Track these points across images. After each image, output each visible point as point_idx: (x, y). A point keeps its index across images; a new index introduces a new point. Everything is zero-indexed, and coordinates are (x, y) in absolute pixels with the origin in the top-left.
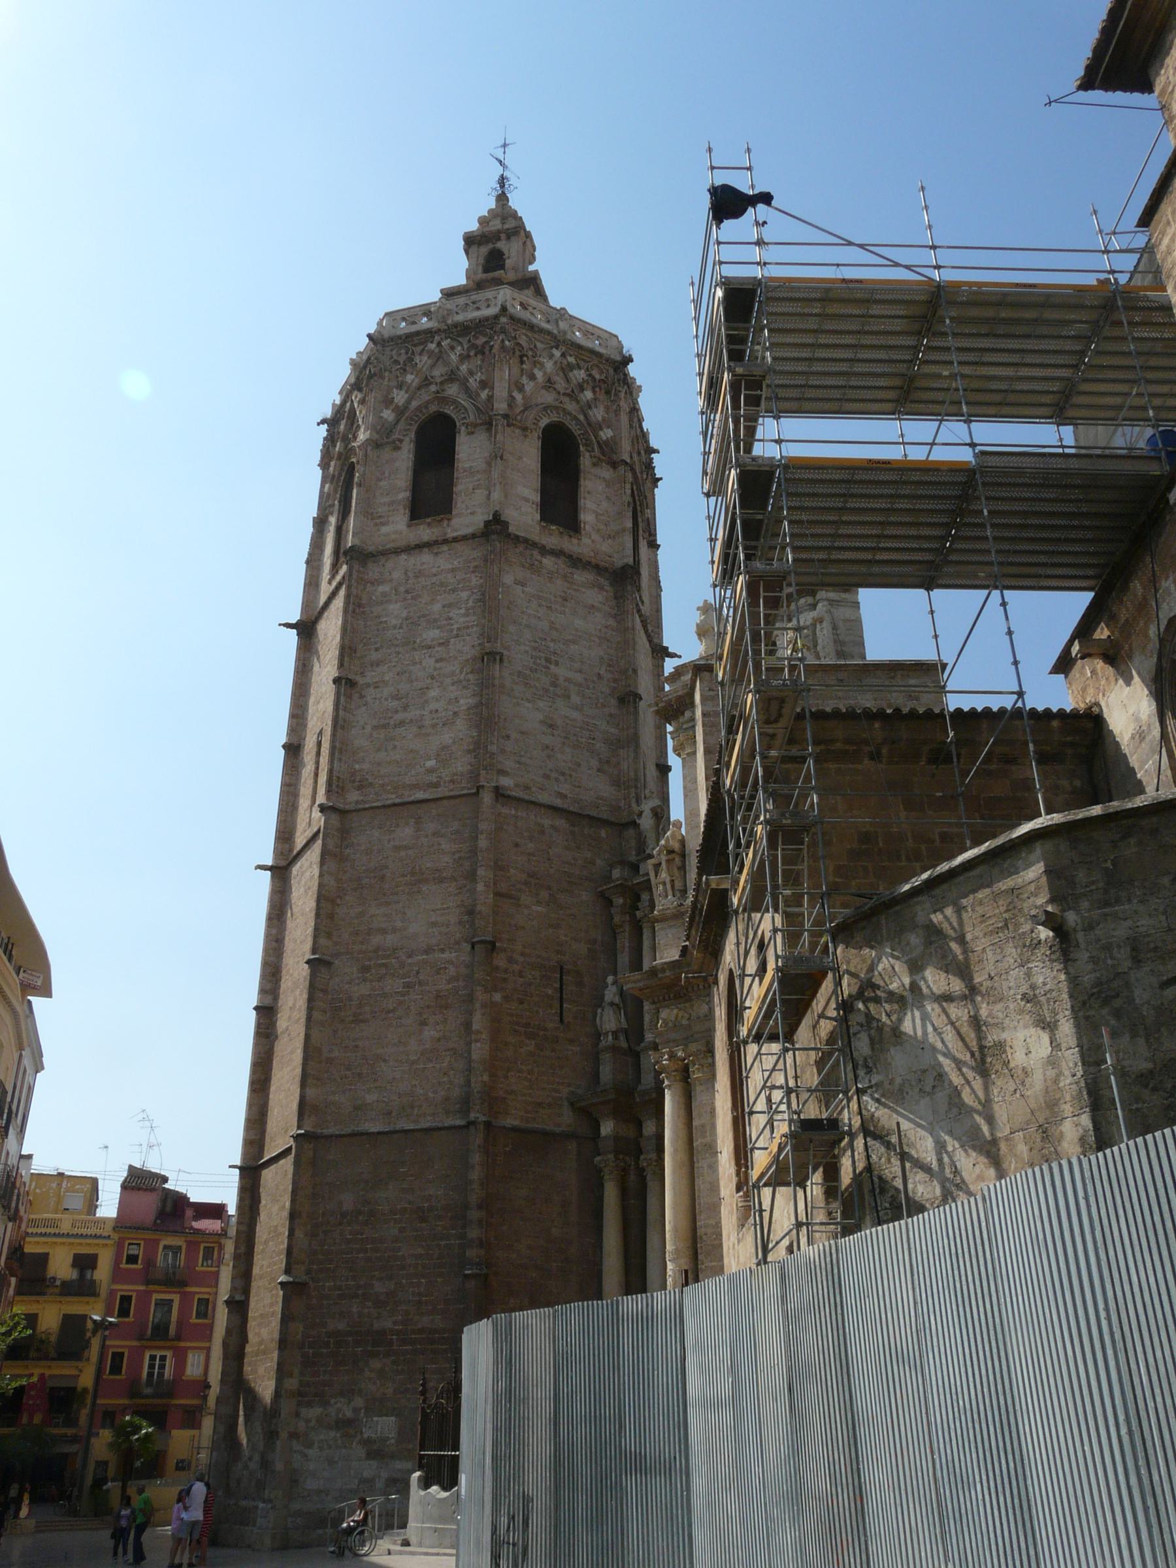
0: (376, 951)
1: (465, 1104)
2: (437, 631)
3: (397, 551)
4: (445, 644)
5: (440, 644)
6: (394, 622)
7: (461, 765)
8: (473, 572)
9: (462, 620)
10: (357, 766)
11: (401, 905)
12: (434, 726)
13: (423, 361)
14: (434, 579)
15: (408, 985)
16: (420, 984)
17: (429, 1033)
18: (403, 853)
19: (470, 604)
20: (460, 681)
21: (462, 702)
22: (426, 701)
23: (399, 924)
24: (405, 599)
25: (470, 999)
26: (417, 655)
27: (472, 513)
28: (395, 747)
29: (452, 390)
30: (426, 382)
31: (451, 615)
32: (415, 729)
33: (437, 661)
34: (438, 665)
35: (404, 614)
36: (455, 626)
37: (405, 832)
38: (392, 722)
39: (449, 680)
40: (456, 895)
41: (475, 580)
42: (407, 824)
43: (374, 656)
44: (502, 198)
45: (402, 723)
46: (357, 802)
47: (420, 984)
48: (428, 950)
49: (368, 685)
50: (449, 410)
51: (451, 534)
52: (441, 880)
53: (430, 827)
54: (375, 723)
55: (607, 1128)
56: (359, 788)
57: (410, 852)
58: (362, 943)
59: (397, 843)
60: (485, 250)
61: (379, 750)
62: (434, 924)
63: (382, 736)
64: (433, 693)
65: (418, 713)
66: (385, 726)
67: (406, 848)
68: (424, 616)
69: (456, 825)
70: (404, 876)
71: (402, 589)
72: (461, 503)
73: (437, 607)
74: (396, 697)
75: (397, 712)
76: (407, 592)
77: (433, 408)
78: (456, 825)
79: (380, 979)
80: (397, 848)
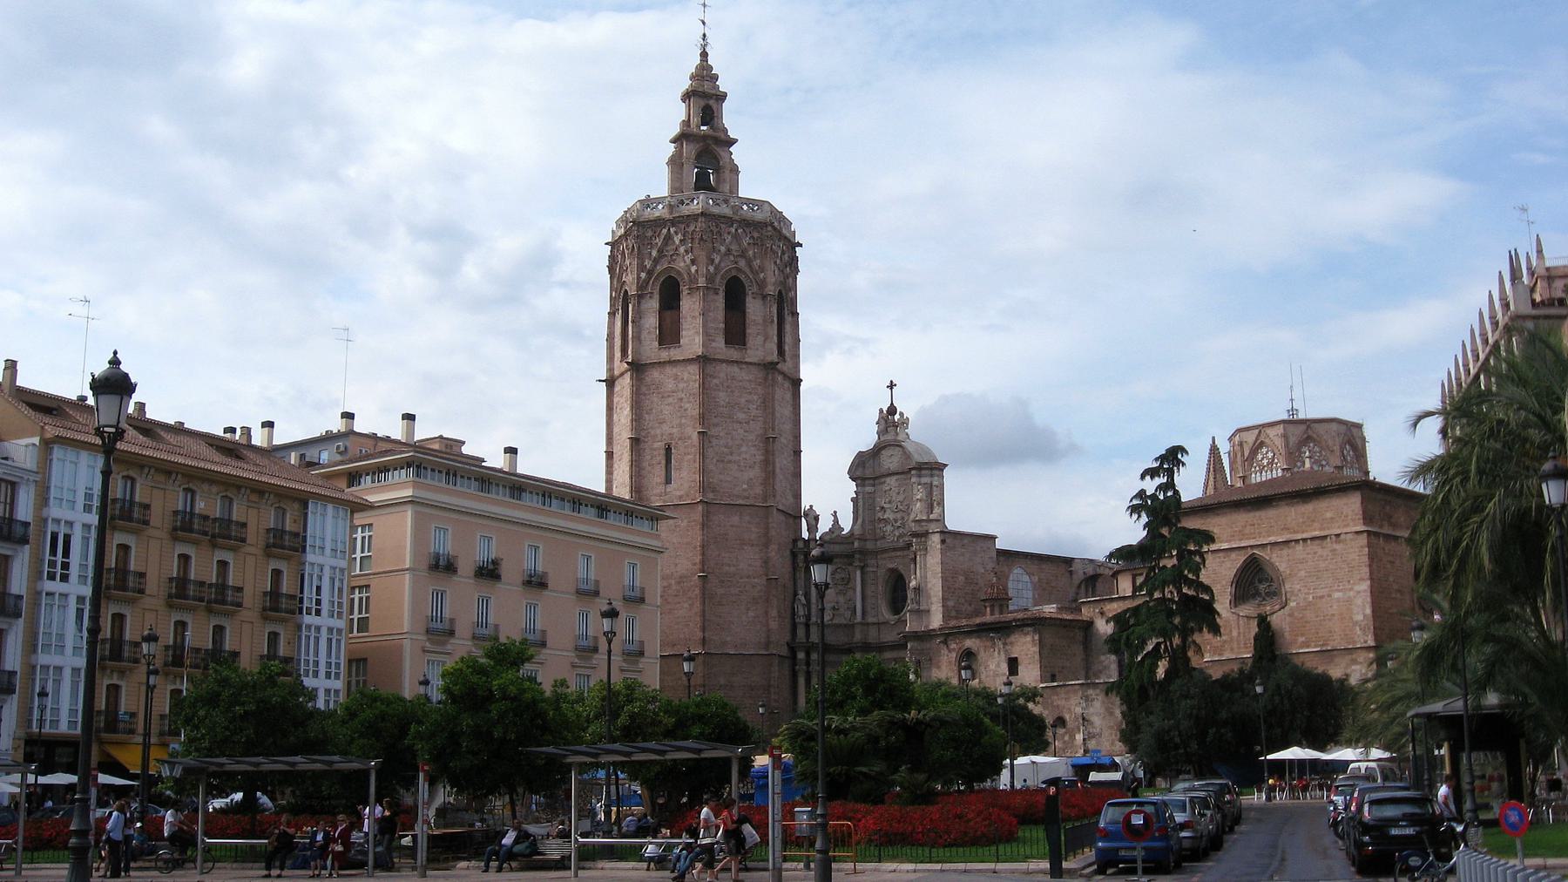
1: (767, 645)
3: (723, 361)
7: (759, 490)
13: (729, 239)
17: (751, 614)
25: (767, 601)
26: (736, 426)
29: (742, 263)
37: (735, 519)
41: (760, 390)
43: (715, 421)
44: (704, 55)
50: (742, 277)
53: (747, 518)
55: (801, 655)
60: (702, 103)
72: (751, 342)
77: (734, 273)
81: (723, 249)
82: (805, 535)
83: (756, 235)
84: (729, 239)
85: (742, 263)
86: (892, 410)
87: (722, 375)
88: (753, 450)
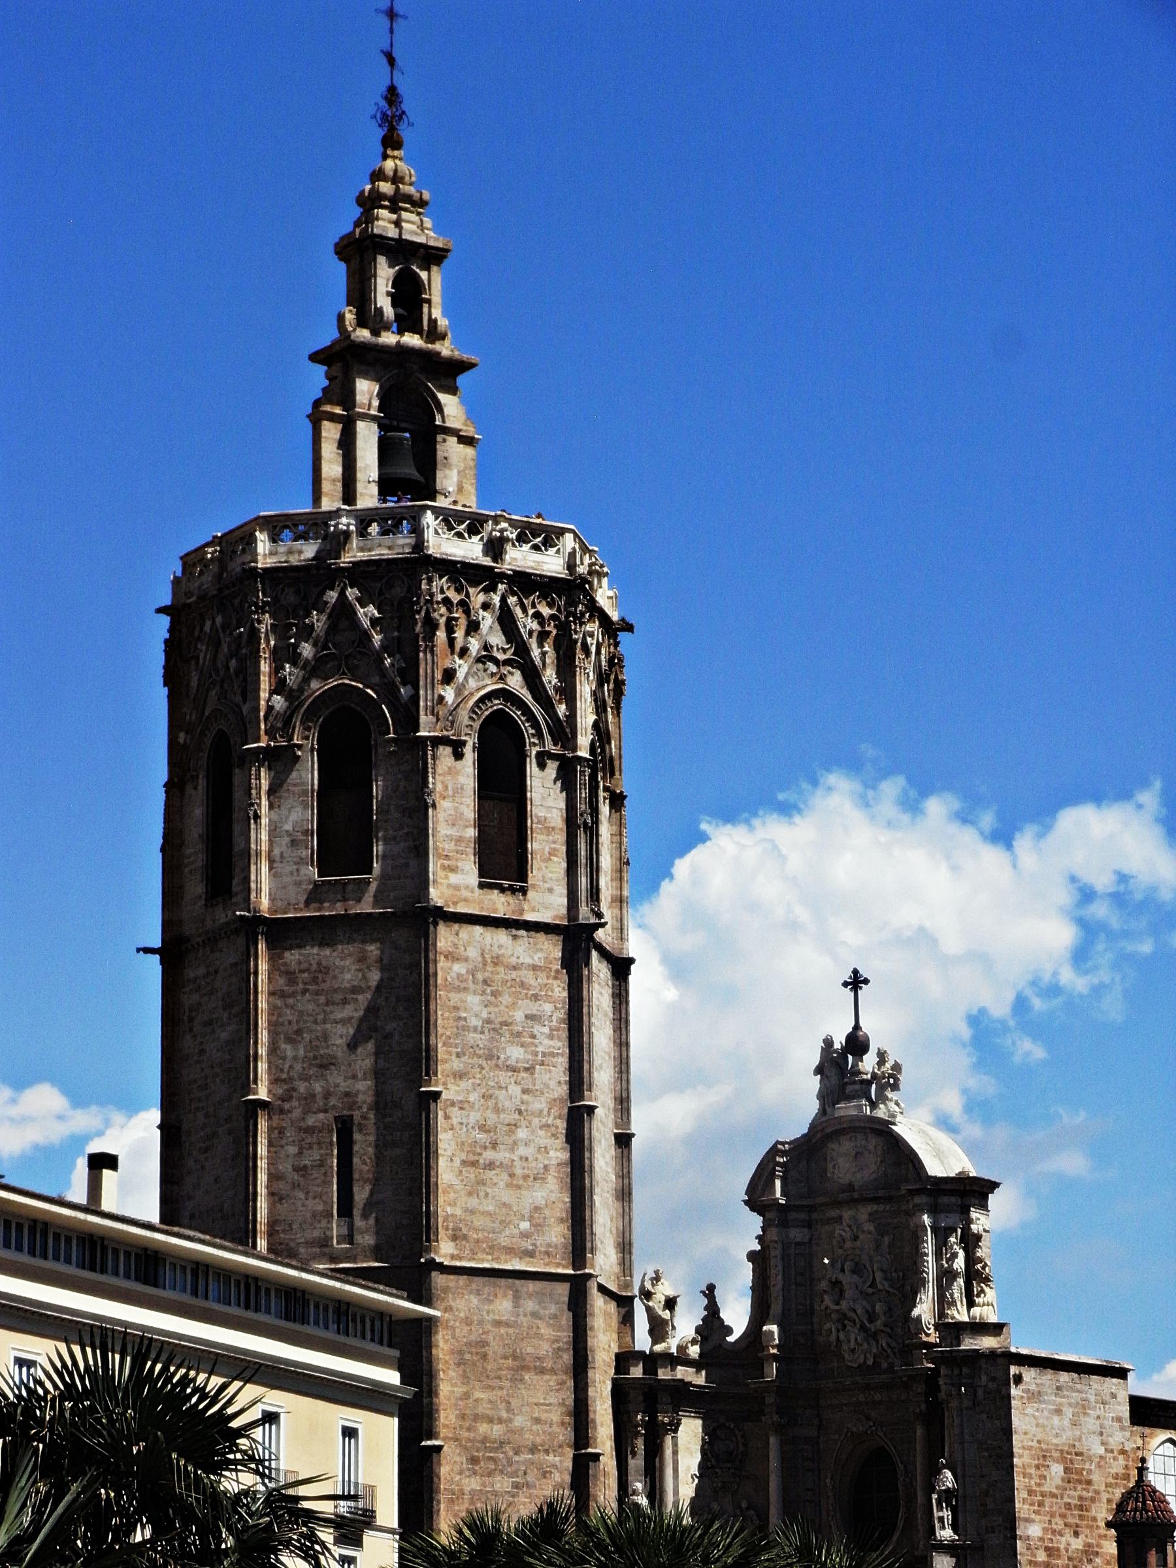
0: (484, 1440)
2: (522, 1050)
4: (530, 1070)
5: (526, 1069)
6: (474, 1022)
7: (557, 1234)
8: (556, 978)
9: (546, 1042)
10: (448, 1209)
11: (505, 1392)
12: (525, 1177)
14: (514, 974)
15: (516, 1486)
16: (528, 1486)
18: (503, 1331)
19: (554, 1023)
20: (548, 1126)
21: (552, 1153)
22: (515, 1143)
23: (504, 1415)
24: (484, 993)
26: (503, 1077)
27: (551, 890)
28: (487, 1195)
30: (486, 656)
31: (535, 1032)
32: (505, 1177)
33: (525, 1091)
34: (525, 1097)
35: (484, 1015)
36: (540, 1049)
37: (503, 1306)
38: (481, 1161)
39: (536, 1121)
40: (557, 1390)
42: (505, 1296)
45: (491, 1166)
46: (453, 1257)
47: (528, 1486)
48: (533, 1449)
49: (453, 1104)
50: (516, 714)
51: (529, 917)
52: (542, 1371)
53: (530, 1305)
54: (463, 1156)
56: (454, 1238)
57: (511, 1331)
58: (469, 1429)
59: (497, 1318)
61: (470, 1194)
62: (537, 1421)
63: (472, 1176)
64: (522, 1134)
65: (507, 1155)
66: (474, 1164)
67: (507, 1324)
68: (505, 1024)
69: (553, 1309)
70: (506, 1358)
71: (480, 976)
73: (519, 1015)
74: (483, 1128)
75: (485, 1148)
76: (485, 982)
77: (497, 704)
78: (553, 1309)
79: (490, 1475)
80: (498, 1323)
81: (474, 645)
82: (642, 1341)
83: (546, 611)
84: (487, 621)
85: (515, 682)
86: (857, 1044)
87: (473, 953)
88: (542, 1138)
